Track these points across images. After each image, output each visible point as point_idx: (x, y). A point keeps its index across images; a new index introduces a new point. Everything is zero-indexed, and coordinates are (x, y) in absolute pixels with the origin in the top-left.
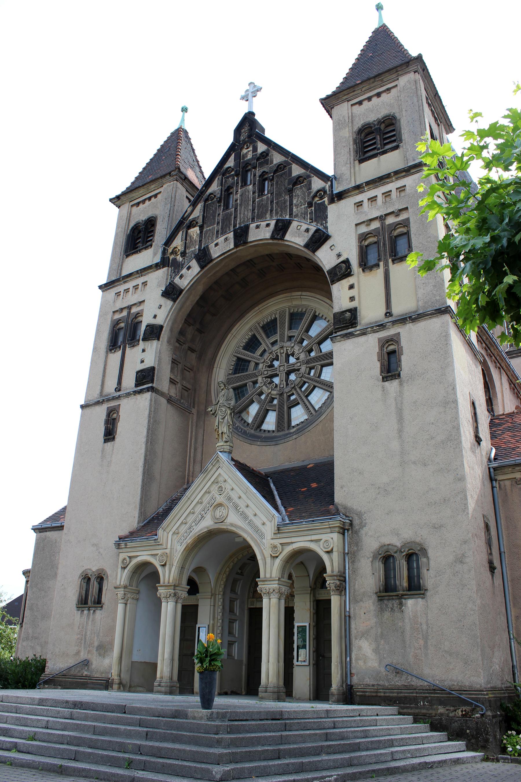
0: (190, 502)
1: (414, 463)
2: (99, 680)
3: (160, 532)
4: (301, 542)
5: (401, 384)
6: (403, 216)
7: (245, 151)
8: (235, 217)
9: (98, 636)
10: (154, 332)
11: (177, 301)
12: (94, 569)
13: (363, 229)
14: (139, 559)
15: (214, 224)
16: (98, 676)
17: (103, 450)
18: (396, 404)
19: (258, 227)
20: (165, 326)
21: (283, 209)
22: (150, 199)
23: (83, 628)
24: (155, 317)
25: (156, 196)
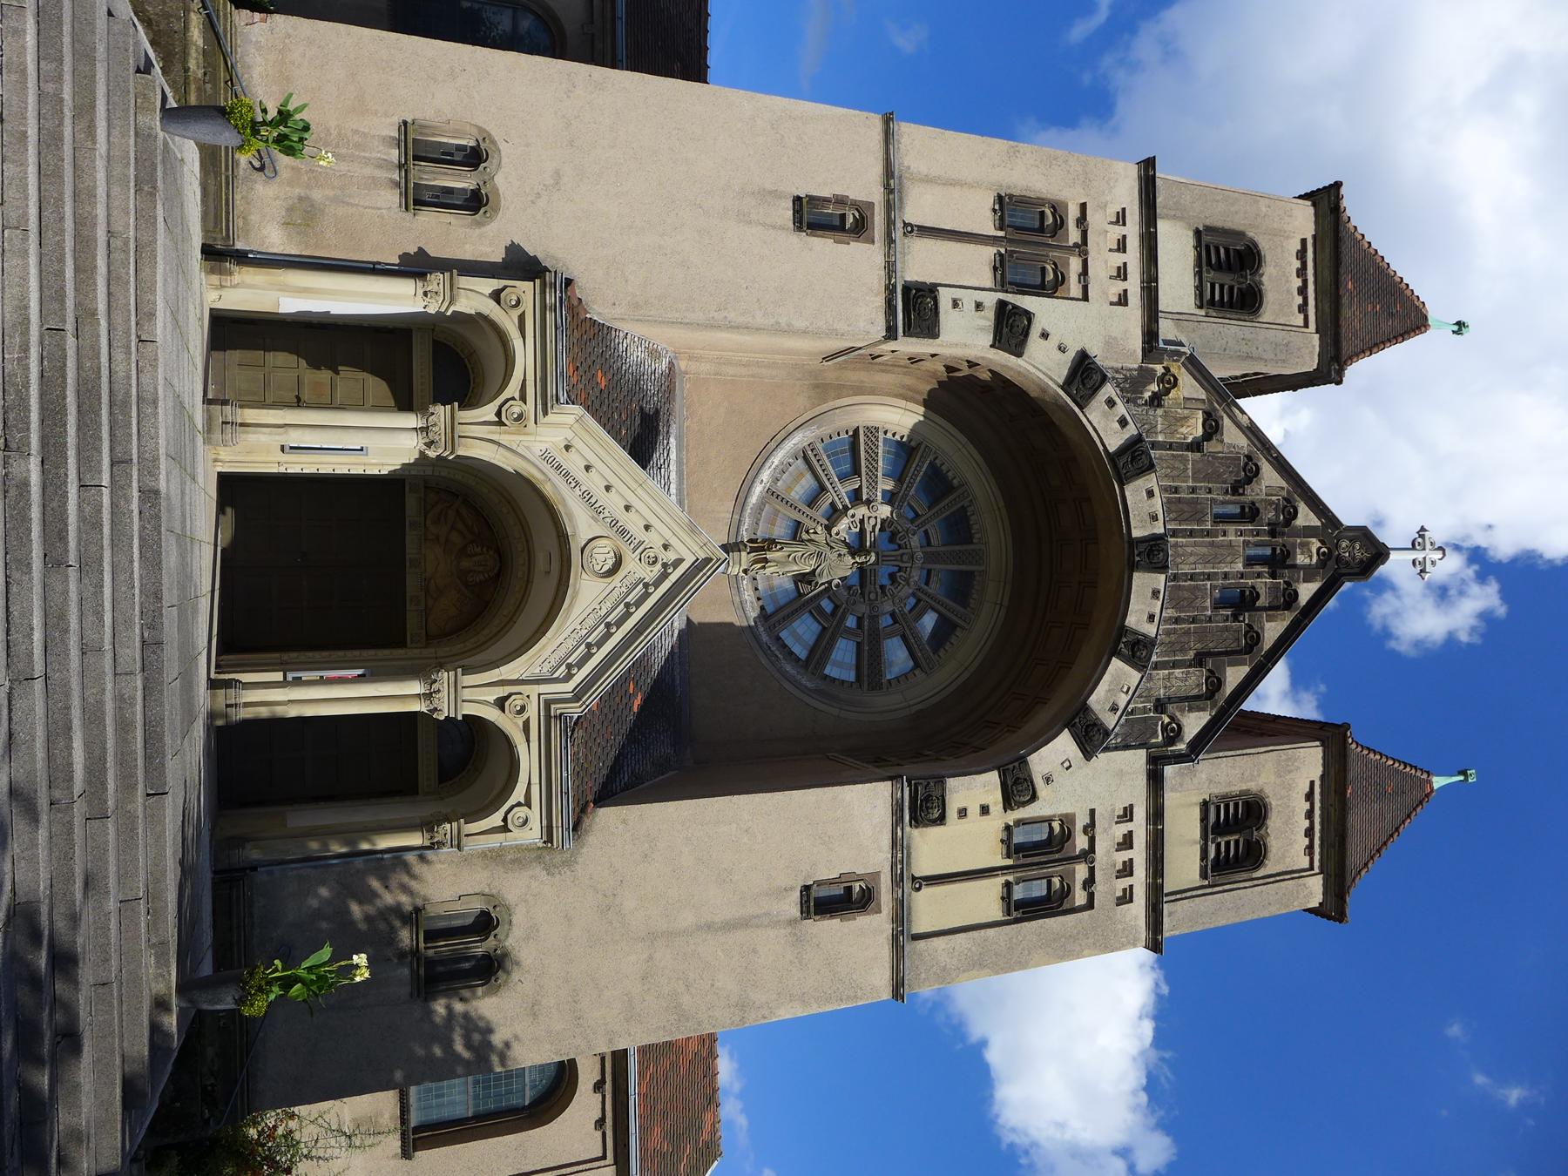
0: (634, 486)
1: (651, 958)
2: (227, 204)
3: (578, 410)
4: (529, 761)
5: (792, 922)
6: (1080, 898)
7: (1315, 544)
8: (1191, 533)
9: (337, 200)
10: (1011, 328)
11: (1062, 393)
12: (499, 180)
14: (517, 343)
15: (1194, 480)
16: (237, 203)
17: (777, 195)
18: (758, 916)
20: (1020, 361)
21: (1172, 648)
23: (357, 146)
24: (1045, 335)
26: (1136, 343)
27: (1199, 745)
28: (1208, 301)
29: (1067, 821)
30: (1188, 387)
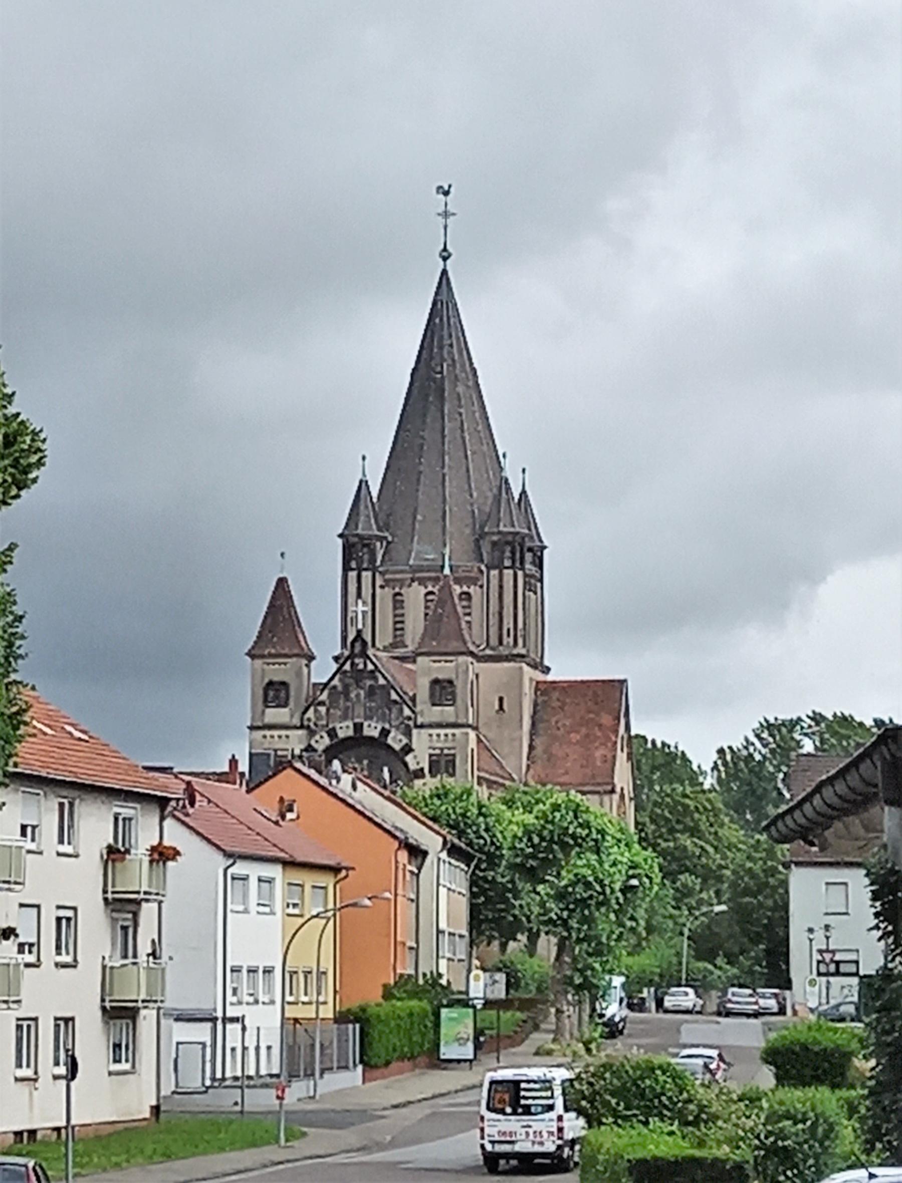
6: (452, 752)
13: (432, 752)
19: (369, 726)
22: (280, 664)
25: (285, 664)
26: (300, 732)
27: (413, 712)
28: (285, 705)
29: (431, 755)
30: (310, 713)
